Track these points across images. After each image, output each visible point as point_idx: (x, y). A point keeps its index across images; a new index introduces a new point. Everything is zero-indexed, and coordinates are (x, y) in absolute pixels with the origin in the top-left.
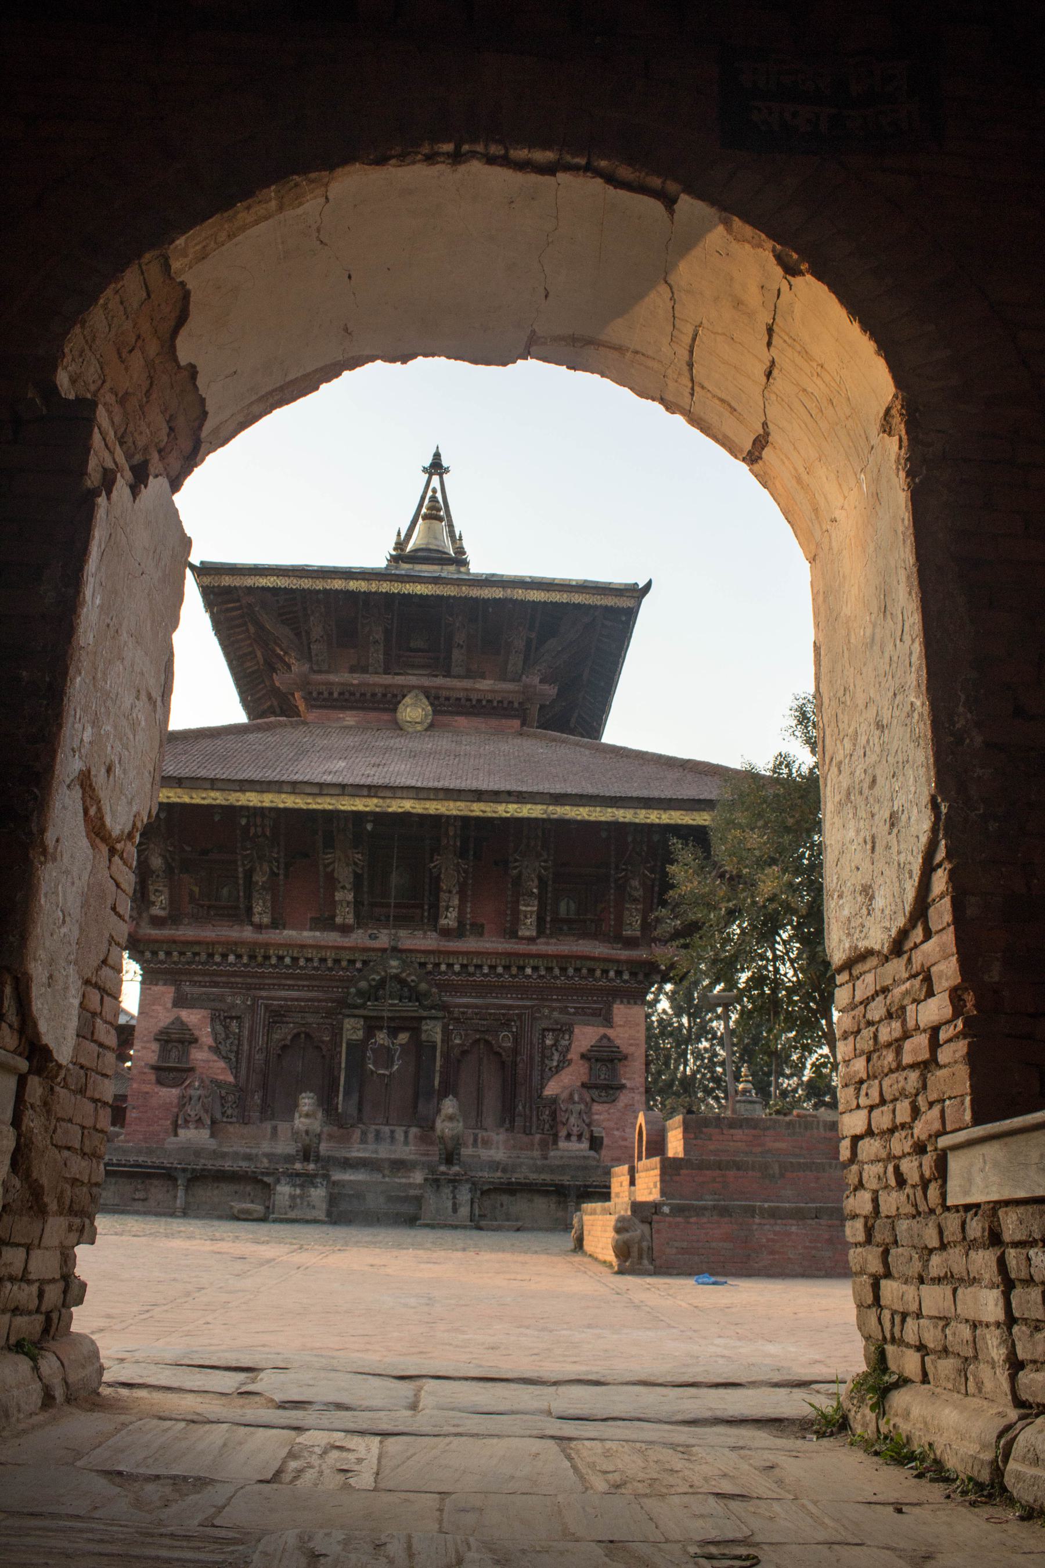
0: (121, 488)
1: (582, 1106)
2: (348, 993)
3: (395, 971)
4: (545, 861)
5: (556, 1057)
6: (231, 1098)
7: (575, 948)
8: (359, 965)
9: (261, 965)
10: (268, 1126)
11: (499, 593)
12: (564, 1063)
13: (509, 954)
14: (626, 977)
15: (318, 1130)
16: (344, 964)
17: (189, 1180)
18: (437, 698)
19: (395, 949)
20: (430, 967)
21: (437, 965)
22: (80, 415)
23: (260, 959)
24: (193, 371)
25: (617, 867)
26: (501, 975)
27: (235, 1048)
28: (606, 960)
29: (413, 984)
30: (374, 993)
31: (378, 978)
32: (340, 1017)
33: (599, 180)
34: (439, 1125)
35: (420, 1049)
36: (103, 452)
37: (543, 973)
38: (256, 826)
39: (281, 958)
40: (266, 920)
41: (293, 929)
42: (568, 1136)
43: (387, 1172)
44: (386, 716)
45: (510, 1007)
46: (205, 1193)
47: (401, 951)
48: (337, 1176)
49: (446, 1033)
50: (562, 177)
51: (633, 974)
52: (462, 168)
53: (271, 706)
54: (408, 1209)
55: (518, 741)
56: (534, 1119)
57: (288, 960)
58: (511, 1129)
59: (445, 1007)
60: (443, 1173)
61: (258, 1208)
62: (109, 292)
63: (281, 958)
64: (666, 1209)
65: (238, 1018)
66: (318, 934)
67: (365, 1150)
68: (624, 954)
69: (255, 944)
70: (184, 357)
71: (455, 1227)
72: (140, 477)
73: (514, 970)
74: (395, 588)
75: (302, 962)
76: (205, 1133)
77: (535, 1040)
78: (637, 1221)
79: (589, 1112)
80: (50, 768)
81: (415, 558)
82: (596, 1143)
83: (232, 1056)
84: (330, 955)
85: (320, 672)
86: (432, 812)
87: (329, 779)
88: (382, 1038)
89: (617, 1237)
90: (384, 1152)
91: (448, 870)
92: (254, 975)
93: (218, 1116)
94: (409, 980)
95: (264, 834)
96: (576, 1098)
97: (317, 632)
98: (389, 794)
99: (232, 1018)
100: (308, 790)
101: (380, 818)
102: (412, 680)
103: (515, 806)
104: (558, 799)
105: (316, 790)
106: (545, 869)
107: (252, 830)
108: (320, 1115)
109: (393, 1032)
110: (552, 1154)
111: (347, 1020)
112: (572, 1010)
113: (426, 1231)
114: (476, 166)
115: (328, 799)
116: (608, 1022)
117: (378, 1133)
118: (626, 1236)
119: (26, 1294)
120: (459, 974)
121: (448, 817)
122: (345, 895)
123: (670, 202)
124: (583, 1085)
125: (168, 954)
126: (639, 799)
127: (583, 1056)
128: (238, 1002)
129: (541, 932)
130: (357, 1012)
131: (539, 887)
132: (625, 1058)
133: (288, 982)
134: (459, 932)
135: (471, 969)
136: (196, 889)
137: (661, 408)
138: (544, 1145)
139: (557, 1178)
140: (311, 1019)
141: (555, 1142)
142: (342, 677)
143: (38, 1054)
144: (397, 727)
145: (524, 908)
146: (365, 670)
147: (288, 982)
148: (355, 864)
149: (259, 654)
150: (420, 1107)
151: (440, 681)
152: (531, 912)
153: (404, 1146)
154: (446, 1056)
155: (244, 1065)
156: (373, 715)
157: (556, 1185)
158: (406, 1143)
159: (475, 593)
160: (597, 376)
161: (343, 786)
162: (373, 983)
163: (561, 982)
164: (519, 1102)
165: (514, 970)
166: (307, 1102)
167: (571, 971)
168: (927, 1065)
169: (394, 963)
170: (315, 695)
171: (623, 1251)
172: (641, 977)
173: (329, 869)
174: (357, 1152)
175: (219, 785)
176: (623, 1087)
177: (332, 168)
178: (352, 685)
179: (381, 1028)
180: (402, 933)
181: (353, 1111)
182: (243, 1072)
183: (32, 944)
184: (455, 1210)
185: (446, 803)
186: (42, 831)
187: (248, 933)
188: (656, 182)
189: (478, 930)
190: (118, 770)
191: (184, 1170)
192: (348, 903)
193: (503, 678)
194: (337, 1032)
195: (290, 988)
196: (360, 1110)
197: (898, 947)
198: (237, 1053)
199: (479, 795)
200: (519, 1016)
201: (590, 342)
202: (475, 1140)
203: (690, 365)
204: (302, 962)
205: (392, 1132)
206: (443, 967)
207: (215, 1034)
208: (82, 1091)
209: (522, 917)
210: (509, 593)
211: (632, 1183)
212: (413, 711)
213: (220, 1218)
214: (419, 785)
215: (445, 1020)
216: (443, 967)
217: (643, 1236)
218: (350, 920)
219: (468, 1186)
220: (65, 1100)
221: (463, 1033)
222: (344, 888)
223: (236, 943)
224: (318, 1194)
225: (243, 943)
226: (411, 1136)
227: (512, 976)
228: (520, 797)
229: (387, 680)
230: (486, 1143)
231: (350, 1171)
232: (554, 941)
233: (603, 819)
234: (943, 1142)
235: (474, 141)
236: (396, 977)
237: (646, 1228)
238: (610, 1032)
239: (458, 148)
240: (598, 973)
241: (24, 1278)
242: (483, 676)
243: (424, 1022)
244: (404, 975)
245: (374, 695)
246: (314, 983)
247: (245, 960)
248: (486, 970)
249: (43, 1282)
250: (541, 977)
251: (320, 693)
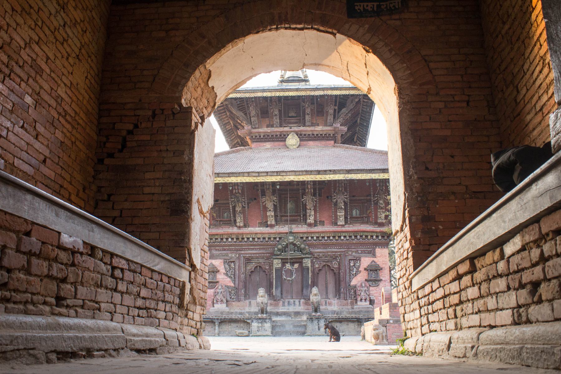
0: (200, 126)
1: (366, 288)
2: (274, 250)
3: (291, 241)
4: (346, 195)
5: (355, 270)
6: (233, 292)
7: (359, 228)
8: (278, 239)
9: (241, 242)
10: (247, 301)
11: (321, 93)
12: (358, 272)
13: (334, 232)
14: (380, 238)
15: (266, 302)
16: (272, 239)
17: (219, 323)
18: (301, 135)
19: (291, 232)
20: (304, 238)
21: (307, 237)
22: (188, 111)
23: (240, 239)
24: (213, 88)
25: (374, 196)
26: (332, 240)
27: (233, 273)
28: (373, 232)
30: (284, 249)
33: (315, 32)
34: (311, 298)
35: (303, 270)
36: (195, 118)
37: (348, 238)
38: (235, 189)
39: (248, 238)
40: (242, 224)
41: (252, 227)
42: (361, 300)
43: (293, 316)
44: (282, 143)
45: (336, 252)
46: (226, 327)
47: (293, 233)
48: (274, 318)
49: (312, 263)
50: (305, 31)
51: (383, 237)
52: (279, 31)
53: (238, 142)
54: (302, 330)
55: (333, 149)
56: (348, 294)
57: (251, 239)
58: (339, 298)
59: (311, 253)
60: (314, 316)
61: (246, 332)
62: (192, 77)
63: (248, 238)
64: (391, 322)
66: (261, 228)
67: (284, 309)
68: (379, 229)
69: (238, 234)
70: (210, 85)
71: (320, 335)
72: (203, 118)
73: (337, 238)
74: (282, 94)
76: (224, 305)
77: (346, 264)
78: (381, 326)
79: (369, 290)
80: (191, 200)
81: (288, 81)
82: (372, 302)
83: (232, 276)
84: (267, 236)
85: (255, 128)
86: (301, 180)
87: (261, 170)
88: (288, 266)
89: (374, 332)
90: (291, 309)
91: (309, 201)
92: (238, 246)
93: (229, 299)
96: (363, 285)
97: (253, 113)
98: (284, 174)
99: (231, 262)
100: (254, 175)
101: (281, 183)
103: (333, 175)
104: (349, 172)
105: (257, 175)
106: (346, 198)
107: (234, 191)
108: (266, 296)
109: (292, 264)
110: (355, 307)
111: (274, 260)
113: (309, 338)
114: (283, 31)
115: (262, 178)
116: (374, 255)
117: (289, 302)
118: (377, 331)
119: (193, 323)
120: (316, 240)
121: (308, 181)
122: (271, 213)
123: (334, 35)
124: (366, 280)
126: (380, 170)
127: (365, 269)
129: (346, 222)
130: (278, 257)
131: (344, 205)
132: (382, 269)
134: (315, 224)
135: (320, 238)
136: (215, 215)
137: (343, 80)
138: (352, 304)
139: (357, 316)
140: (261, 261)
141: (356, 303)
142: (264, 130)
143: (193, 266)
146: (272, 126)
148: (274, 201)
149: (231, 123)
150: (304, 291)
151: (302, 128)
153: (298, 306)
154: (313, 272)
155: (237, 279)
156: (277, 143)
157: (357, 318)
158: (300, 305)
159: (312, 93)
160: (324, 72)
161: (267, 172)
164: (341, 288)
165: (337, 238)
166: (261, 291)
167: (359, 237)
168: (407, 258)
169: (291, 238)
170: (254, 137)
171: (377, 337)
172: (386, 238)
174: (281, 309)
175: (220, 175)
176: (381, 280)
177: (245, 36)
179: (287, 263)
180: (293, 226)
181: (279, 294)
182: (237, 282)
183: (191, 241)
184: (319, 329)
185: (306, 176)
186: (191, 215)
187: (235, 230)
188: (330, 30)
189: (322, 223)
190: (204, 196)
191: (218, 319)
193: (326, 125)
194: (271, 265)
195: (252, 249)
196: (282, 294)
197: (402, 230)
198: (234, 275)
199: (319, 172)
200: (340, 255)
201: (319, 65)
202: (326, 303)
203: (348, 70)
204: (256, 240)
205: (294, 301)
206: (310, 238)
207: (226, 269)
208: (202, 276)
210: (326, 93)
211: (381, 314)
212: (292, 140)
213: (232, 336)
214: (296, 170)
216: (310, 238)
217: (383, 331)
218: (273, 222)
219: (323, 320)
220: (199, 278)
222: (270, 210)
223: (231, 234)
224: (268, 325)
225: (233, 234)
226: (301, 302)
227: (336, 240)
228: (335, 172)
229: (281, 129)
230: (330, 304)
231: (279, 317)
232: (351, 226)
233: (367, 178)
234: (411, 276)
235: (281, 24)
236: (292, 243)
237: (384, 328)
238: (375, 259)
239: (277, 26)
240: (369, 237)
241: (193, 320)
242: (318, 125)
245: (277, 135)
246: (262, 247)
247: (235, 240)
248: (326, 238)
249: (197, 321)
250: (347, 240)
251: (256, 136)
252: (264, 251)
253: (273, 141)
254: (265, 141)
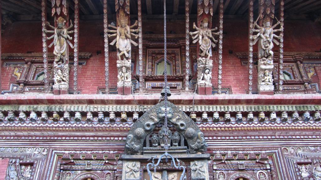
8: (136, 116)
29: (182, 128)
31: (151, 123)
32: (120, 162)
39: (72, 114)
57: (78, 115)
63: (72, 114)
65: (31, 164)
94: (179, 123)
95: (62, 14)
99: (26, 165)
106: (278, 33)
111: (126, 164)
112: (313, 148)
128: (36, 153)
130: (134, 157)
133: (78, 134)
134: (214, 90)
140: (95, 165)
145: (263, 67)
147: (78, 134)
152: (269, 70)
162: (148, 128)
173: (112, 44)
192: (127, 68)
209: (261, 75)
215: (210, 162)
218: (128, 83)
221: (225, 172)
222: (123, 57)
243: (192, 163)
244: (174, 120)
247: (44, 115)
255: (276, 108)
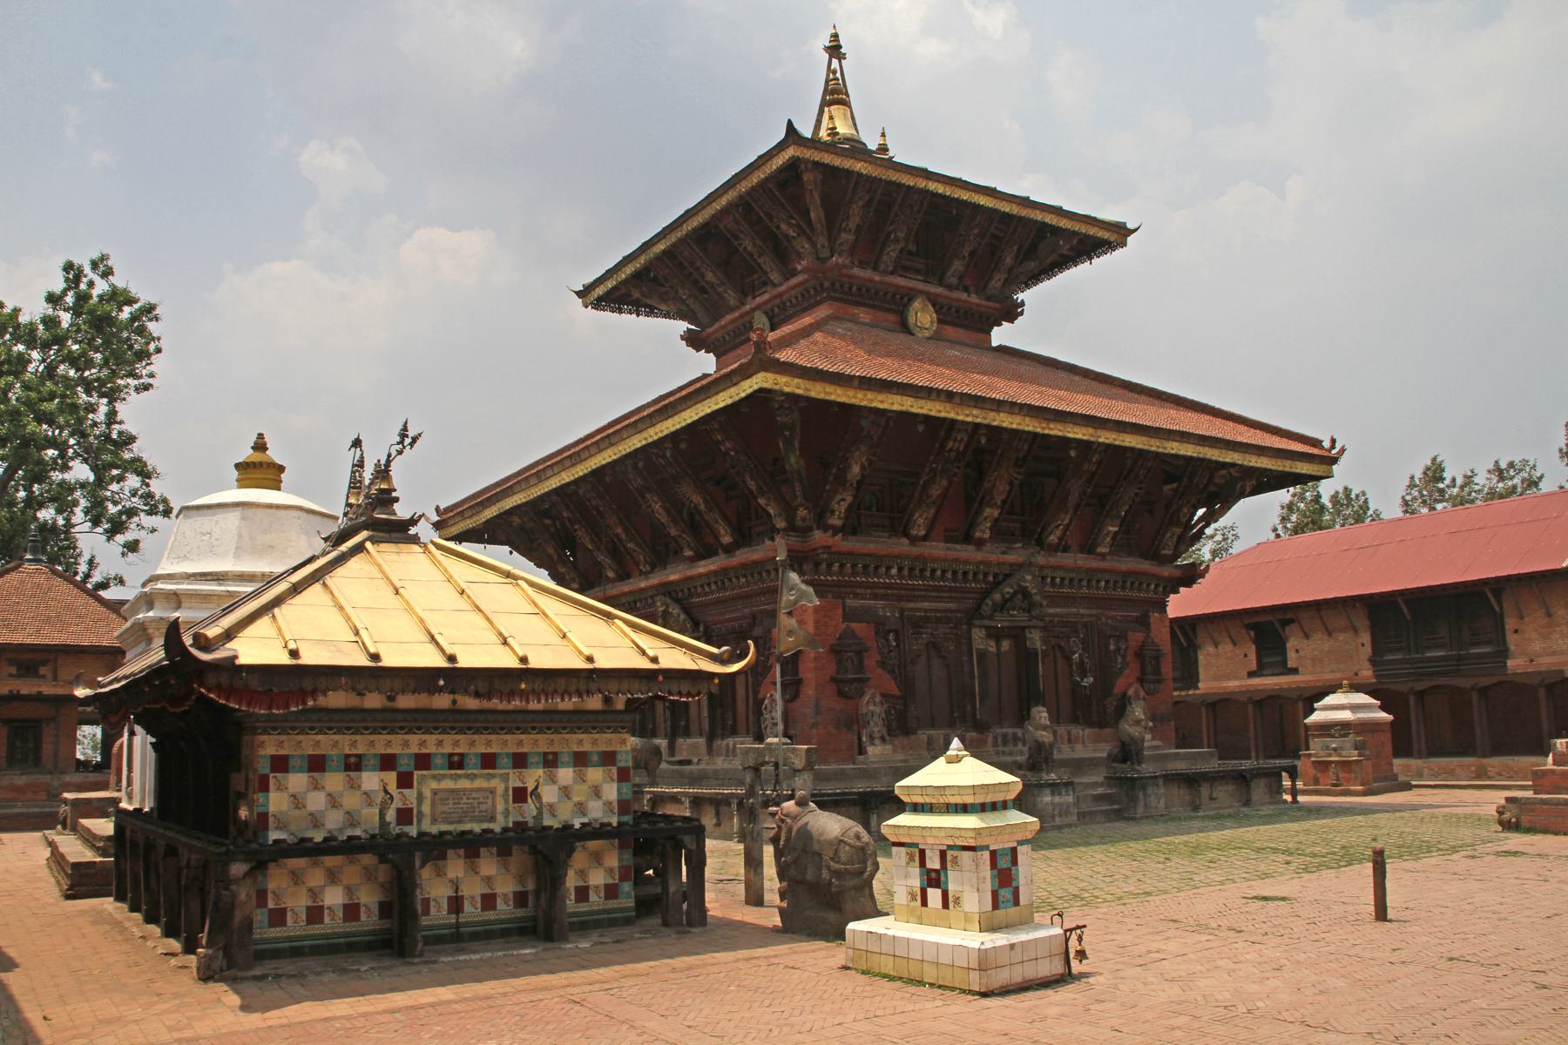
39: (933, 571)
40: (923, 533)
44: (892, 317)
57: (939, 573)
69: (918, 557)
75: (949, 575)
99: (889, 631)
102: (920, 286)
125: (842, 566)
144: (905, 328)
156: (881, 314)
163: (1119, 592)
169: (1029, 577)
178: (872, 281)
187: (902, 546)
212: (923, 316)
218: (987, 535)
247: (906, 573)
252: (951, 606)
253: (873, 307)
254: (857, 304)
255: (1107, 576)
